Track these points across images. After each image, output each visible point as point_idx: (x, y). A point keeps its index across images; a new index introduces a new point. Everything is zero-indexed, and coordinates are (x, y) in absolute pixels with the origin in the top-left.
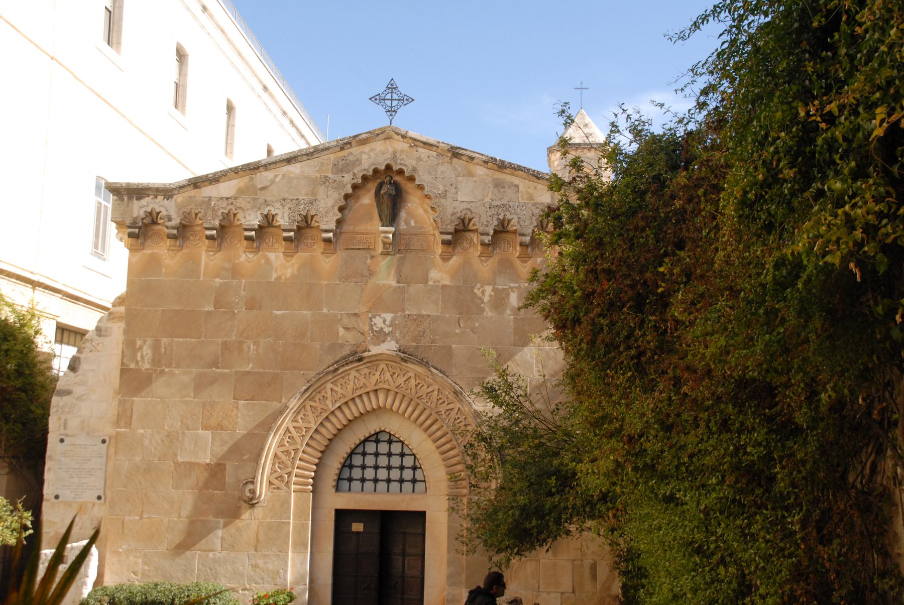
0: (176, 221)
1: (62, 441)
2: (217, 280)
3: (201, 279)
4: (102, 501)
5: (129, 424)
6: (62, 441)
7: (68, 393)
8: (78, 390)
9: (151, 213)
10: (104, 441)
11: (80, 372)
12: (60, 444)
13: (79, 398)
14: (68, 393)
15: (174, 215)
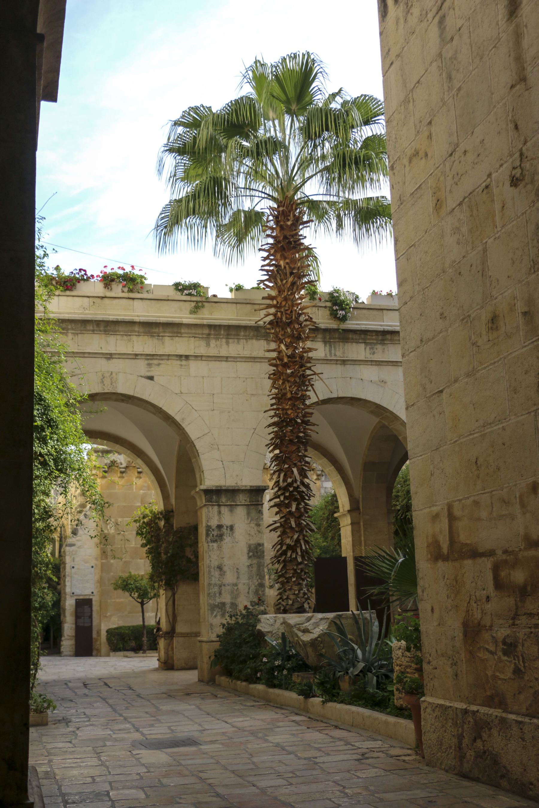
0: (124, 465)
1: (73, 567)
2: (141, 491)
3: (134, 490)
4: (94, 594)
5: (106, 558)
6: (73, 567)
7: (74, 545)
8: (78, 544)
9: (112, 462)
10: (92, 567)
11: (79, 535)
12: (73, 569)
13: (79, 547)
14: (74, 545)
15: (123, 462)
